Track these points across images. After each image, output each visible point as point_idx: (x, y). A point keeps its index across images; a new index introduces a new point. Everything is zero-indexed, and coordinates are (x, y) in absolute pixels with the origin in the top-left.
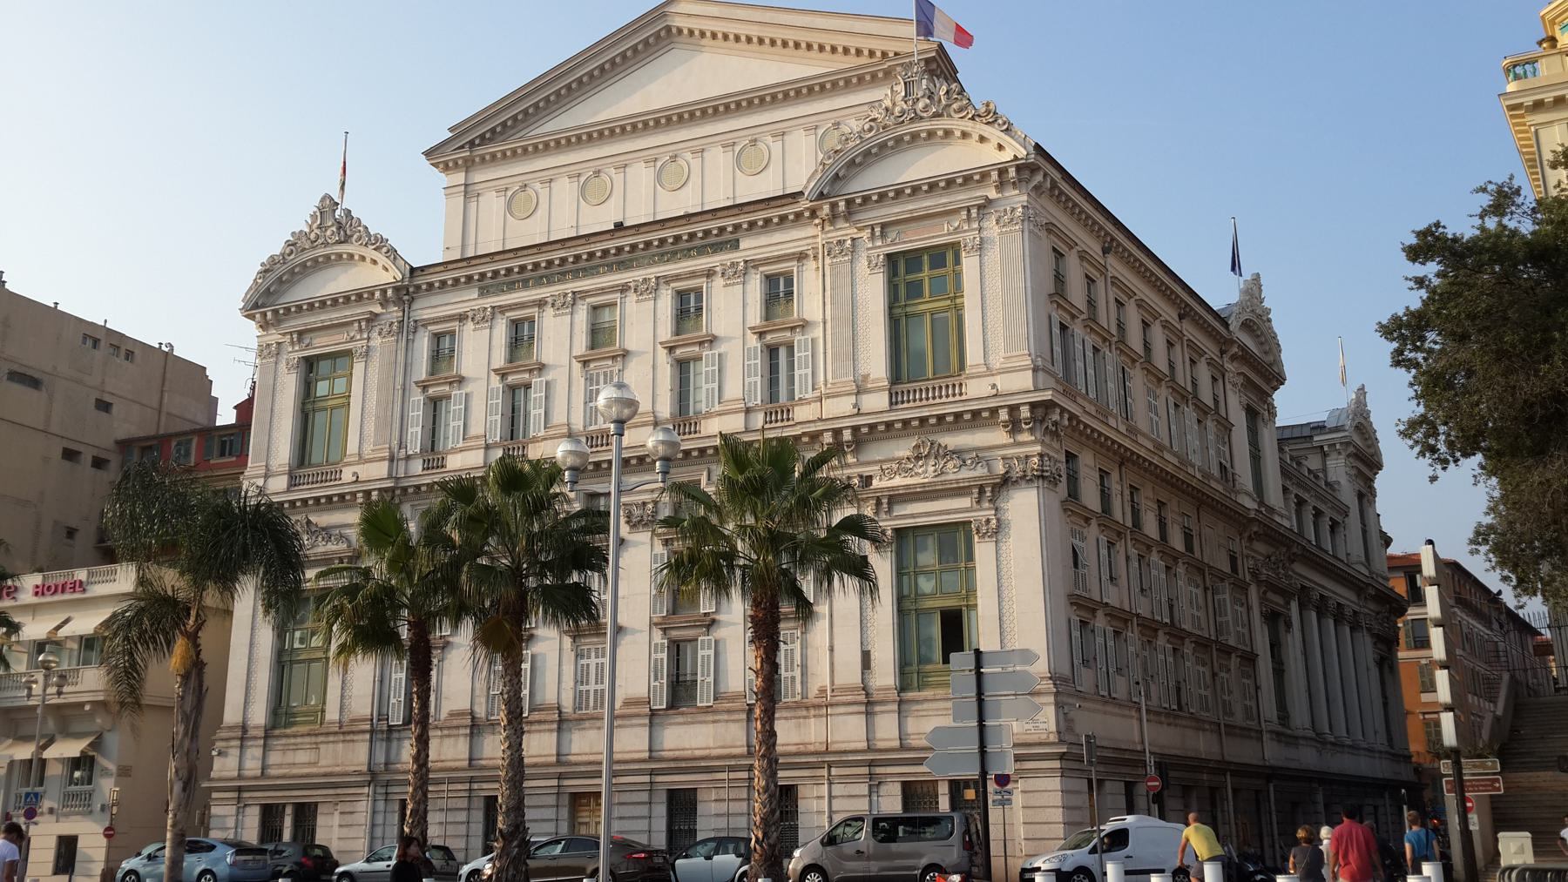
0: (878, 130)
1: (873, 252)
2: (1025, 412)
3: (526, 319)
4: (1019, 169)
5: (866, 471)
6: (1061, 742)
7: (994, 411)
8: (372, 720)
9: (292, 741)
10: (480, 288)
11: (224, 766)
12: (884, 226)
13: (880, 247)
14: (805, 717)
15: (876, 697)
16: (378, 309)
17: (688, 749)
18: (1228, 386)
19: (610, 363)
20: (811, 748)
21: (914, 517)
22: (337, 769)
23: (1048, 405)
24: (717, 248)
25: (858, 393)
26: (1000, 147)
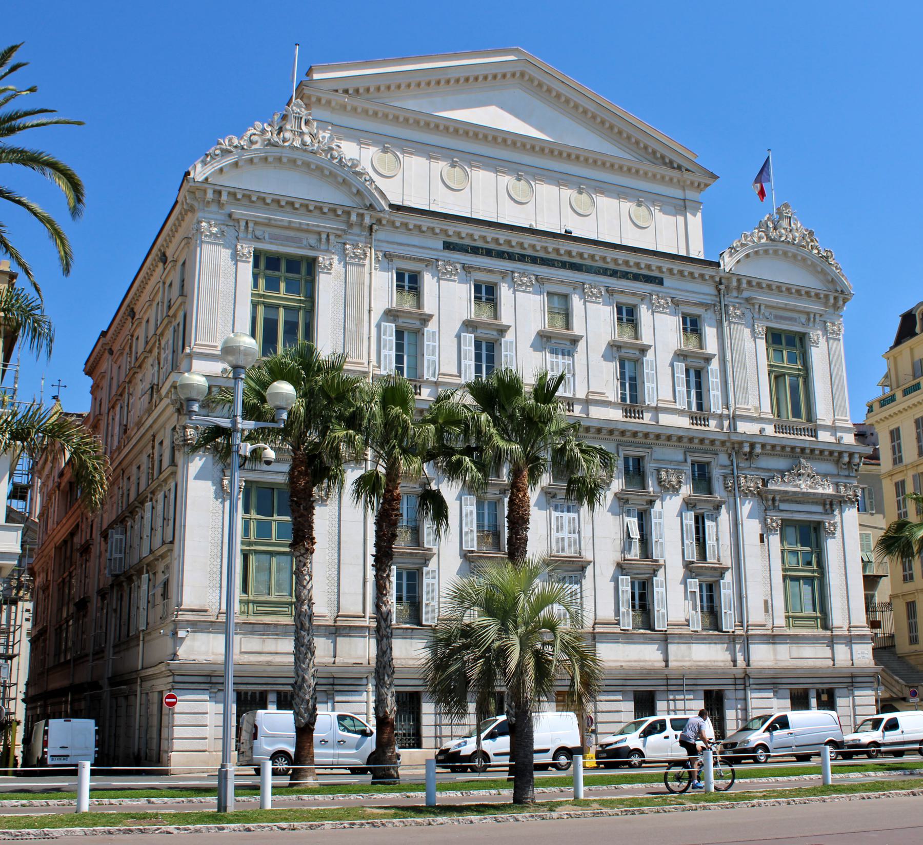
10: (445, 243)
24: (648, 279)
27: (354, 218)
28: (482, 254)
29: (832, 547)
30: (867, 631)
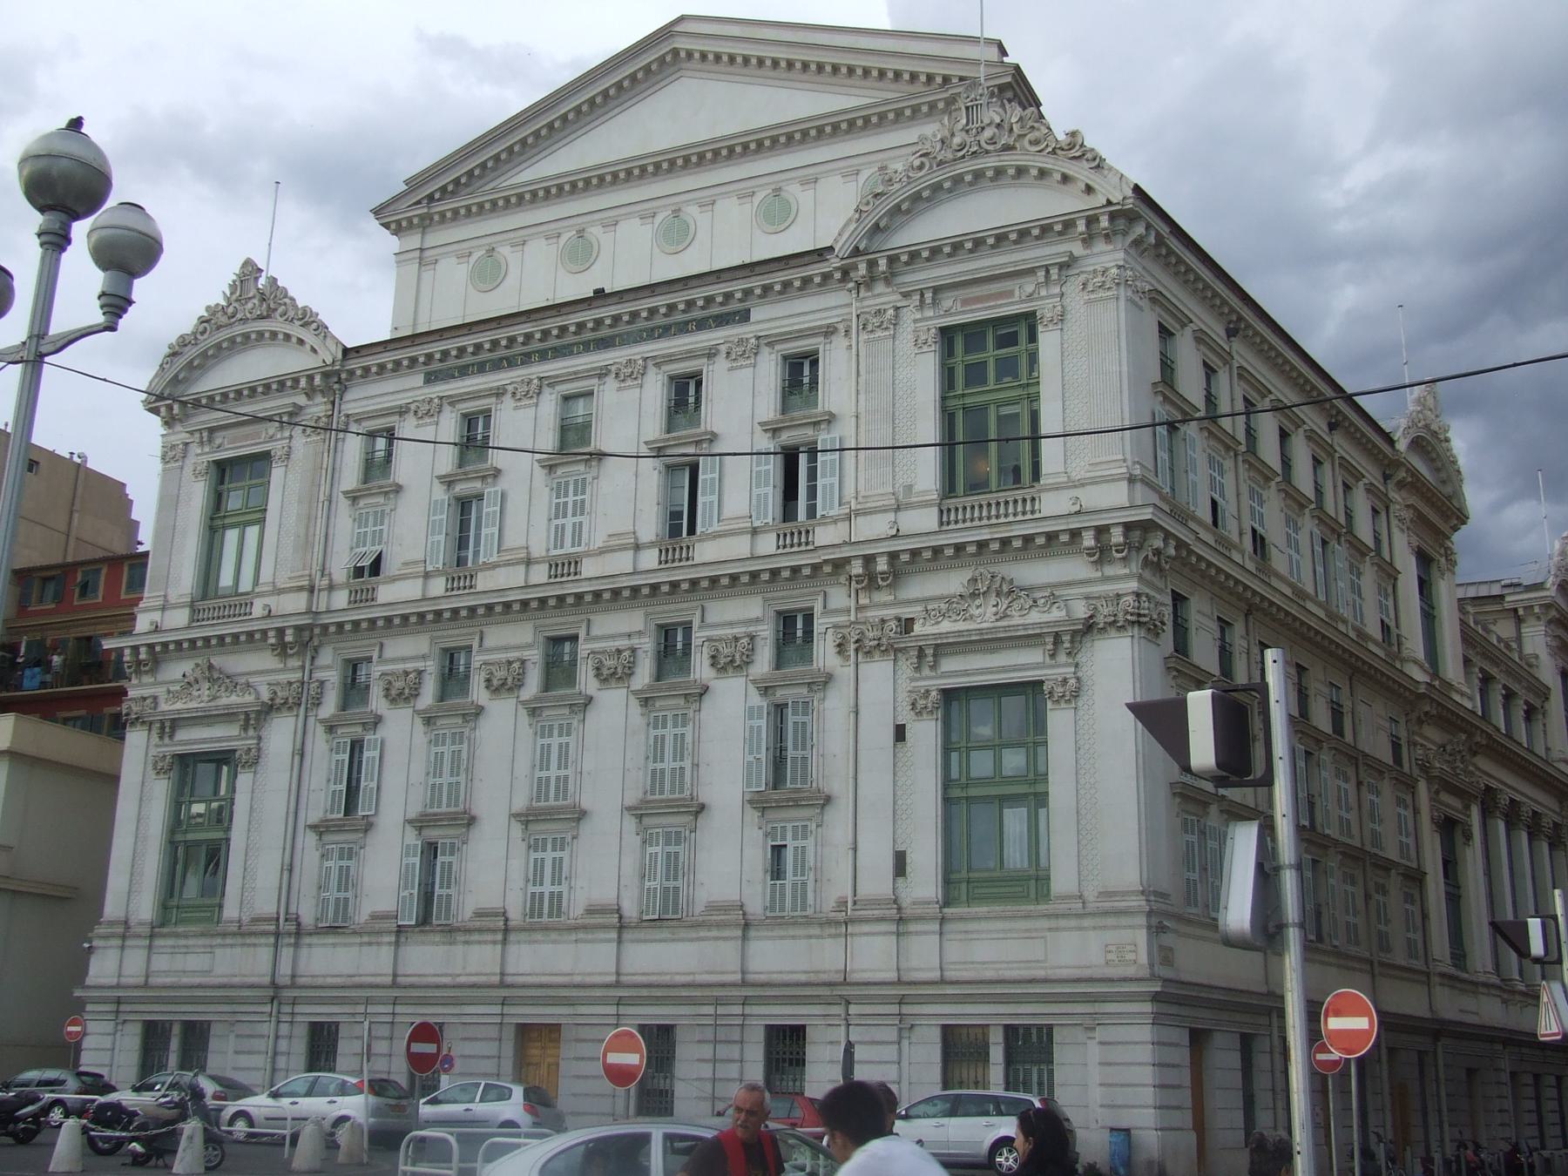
0: (931, 167)
1: (919, 323)
2: (1117, 536)
3: (481, 412)
4: (1113, 217)
5: (906, 612)
6: (1153, 977)
7: (1075, 534)
8: (278, 919)
9: (182, 942)
11: (103, 968)
12: (936, 290)
13: (930, 318)
14: (818, 937)
15: (908, 912)
16: (301, 400)
17: (667, 974)
18: (1394, 522)
20: (824, 978)
21: (968, 675)
22: (236, 980)
23: (1147, 527)
24: (722, 320)
25: (898, 509)
26: (1089, 189)
28: (473, 373)
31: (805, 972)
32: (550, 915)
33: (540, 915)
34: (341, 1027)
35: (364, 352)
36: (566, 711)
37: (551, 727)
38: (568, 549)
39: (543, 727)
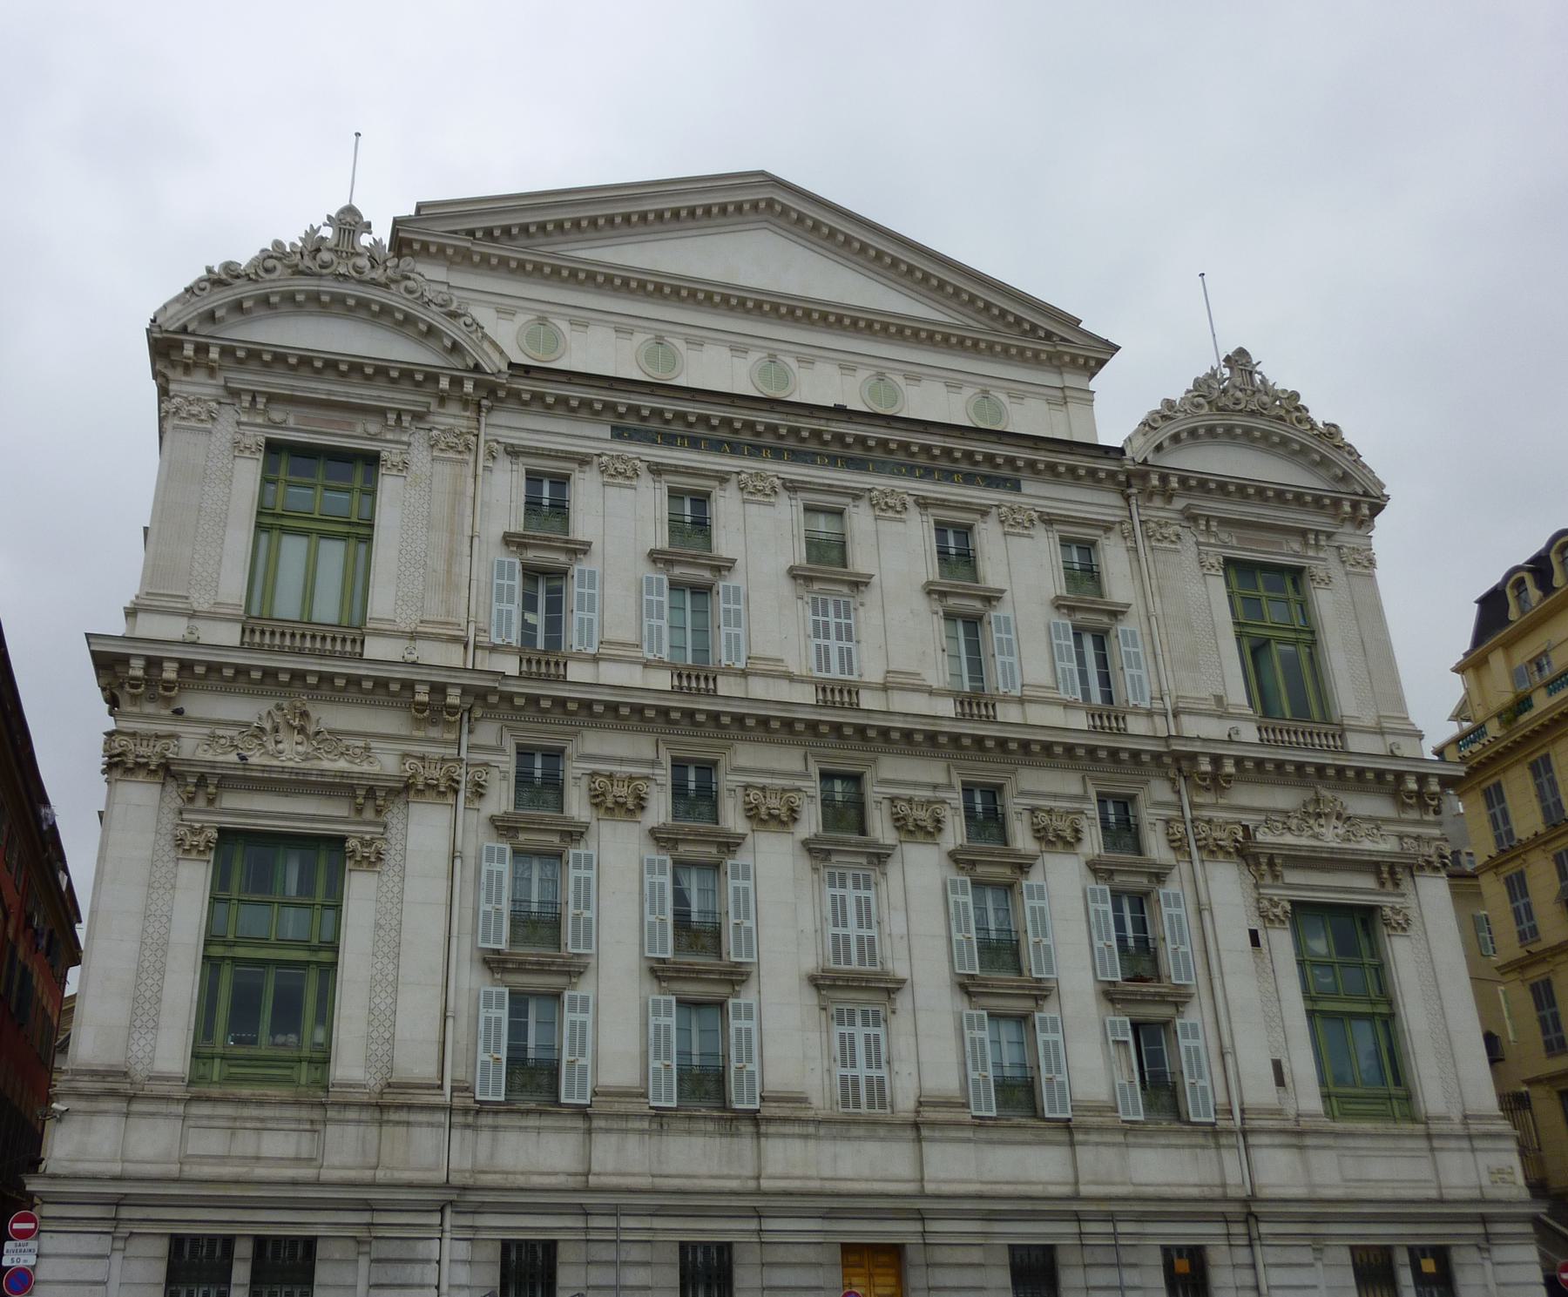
5: (1249, 819)
8: (441, 1087)
10: (614, 428)
19: (845, 590)
20: (1232, 1192)
27: (444, 383)
28: (682, 445)
29: (1401, 953)
30: (1504, 1126)
31: (1195, 1185)
32: (871, 1105)
33: (857, 1105)
34: (561, 1246)
35: (533, 374)
36: (863, 860)
37: (843, 877)
38: (835, 673)
39: (832, 875)
